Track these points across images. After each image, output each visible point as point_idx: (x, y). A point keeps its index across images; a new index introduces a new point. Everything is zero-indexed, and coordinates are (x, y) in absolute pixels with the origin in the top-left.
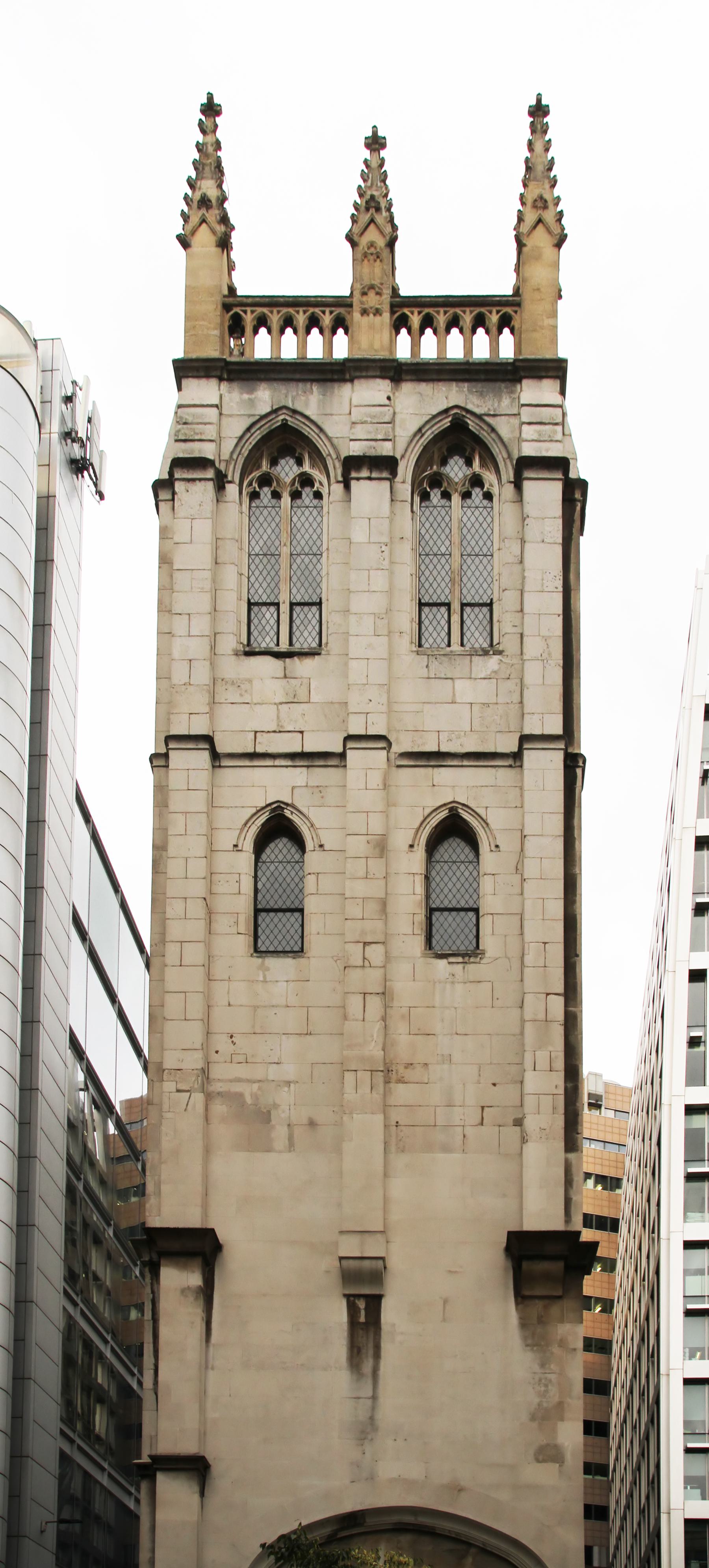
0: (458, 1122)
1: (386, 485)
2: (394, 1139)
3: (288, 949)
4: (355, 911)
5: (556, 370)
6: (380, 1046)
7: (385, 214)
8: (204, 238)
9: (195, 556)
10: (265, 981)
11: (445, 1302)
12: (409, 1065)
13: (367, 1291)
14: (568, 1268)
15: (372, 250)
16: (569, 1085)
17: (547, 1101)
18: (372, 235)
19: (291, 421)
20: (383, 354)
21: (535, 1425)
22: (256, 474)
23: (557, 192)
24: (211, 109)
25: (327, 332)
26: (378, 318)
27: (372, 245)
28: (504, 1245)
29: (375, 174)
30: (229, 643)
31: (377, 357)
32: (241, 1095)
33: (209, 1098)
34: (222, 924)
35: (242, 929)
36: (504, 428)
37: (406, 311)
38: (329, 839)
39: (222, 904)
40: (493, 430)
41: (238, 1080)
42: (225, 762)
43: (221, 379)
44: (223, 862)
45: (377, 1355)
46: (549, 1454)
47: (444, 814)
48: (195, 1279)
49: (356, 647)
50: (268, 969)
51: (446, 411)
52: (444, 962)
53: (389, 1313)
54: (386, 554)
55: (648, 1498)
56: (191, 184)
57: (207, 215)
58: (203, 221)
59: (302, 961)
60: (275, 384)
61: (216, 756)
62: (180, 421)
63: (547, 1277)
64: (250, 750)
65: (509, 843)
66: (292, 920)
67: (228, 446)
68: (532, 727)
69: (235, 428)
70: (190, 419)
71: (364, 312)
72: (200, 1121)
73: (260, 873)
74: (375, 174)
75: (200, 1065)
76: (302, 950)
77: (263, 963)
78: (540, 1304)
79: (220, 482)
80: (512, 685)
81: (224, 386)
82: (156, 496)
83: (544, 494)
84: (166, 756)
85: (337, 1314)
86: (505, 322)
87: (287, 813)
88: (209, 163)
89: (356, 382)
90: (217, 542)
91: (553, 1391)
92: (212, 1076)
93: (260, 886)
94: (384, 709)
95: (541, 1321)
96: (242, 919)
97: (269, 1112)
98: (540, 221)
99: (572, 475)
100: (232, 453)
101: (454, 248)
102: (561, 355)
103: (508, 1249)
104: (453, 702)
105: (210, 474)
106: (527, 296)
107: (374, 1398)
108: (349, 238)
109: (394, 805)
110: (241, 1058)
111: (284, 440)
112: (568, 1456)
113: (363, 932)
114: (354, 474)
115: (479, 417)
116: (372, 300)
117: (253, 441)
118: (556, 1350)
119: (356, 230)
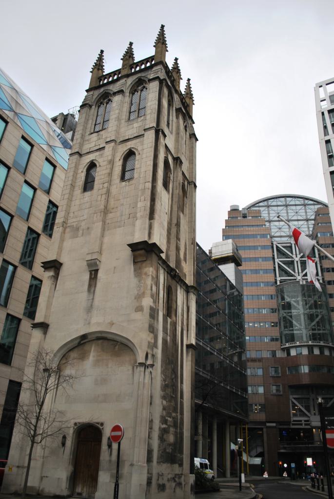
11: (115, 268)
12: (113, 208)
16: (152, 203)
35: (80, 188)
45: (95, 286)
46: (139, 309)
53: (100, 274)
78: (140, 263)
85: (87, 277)
91: (142, 288)
95: (140, 268)
96: (81, 186)
107: (93, 299)
112: (145, 309)
118: (144, 276)
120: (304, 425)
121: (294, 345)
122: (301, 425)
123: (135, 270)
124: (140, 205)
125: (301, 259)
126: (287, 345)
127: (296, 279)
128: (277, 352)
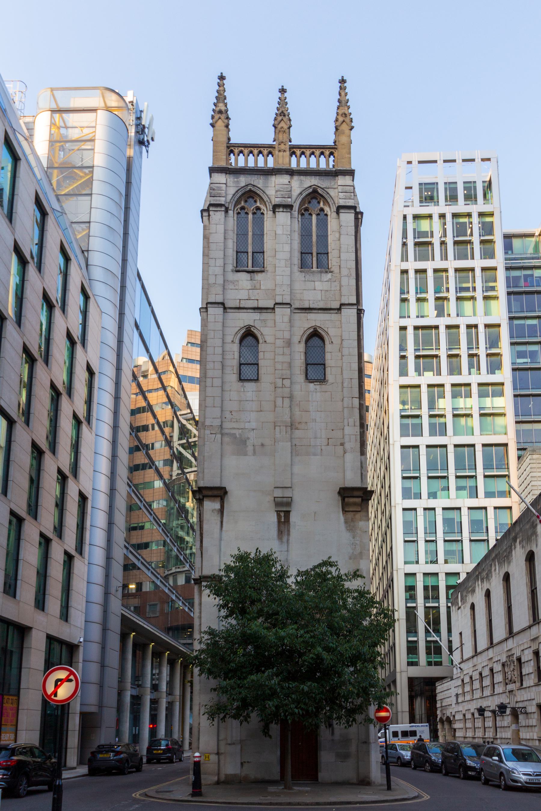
0: (318, 444)
1: (289, 214)
2: (295, 450)
3: (252, 378)
4: (279, 366)
5: (351, 173)
6: (289, 417)
7: (287, 117)
8: (220, 124)
9: (218, 237)
10: (244, 391)
11: (315, 513)
13: (284, 509)
14: (362, 500)
15: (282, 130)
16: (361, 430)
17: (353, 438)
18: (282, 124)
19: (253, 189)
20: (286, 167)
21: (351, 561)
22: (239, 206)
23: (350, 111)
24: (222, 78)
25: (265, 156)
26: (285, 153)
27: (282, 127)
28: (338, 491)
29: (282, 102)
30: (230, 267)
31: (284, 167)
32: (235, 434)
33: (222, 434)
34: (228, 370)
35: (235, 372)
36: (332, 193)
37: (295, 150)
38: (269, 339)
39: (228, 363)
40: (328, 193)
41: (234, 429)
42: (228, 310)
43: (226, 173)
44: (228, 347)
45: (289, 534)
47: (312, 330)
48: (217, 506)
49: (279, 271)
50: (245, 387)
51: (311, 186)
52: (313, 384)
53: (294, 518)
54: (289, 238)
55: (387, 562)
56: (215, 105)
57: (221, 115)
58: (220, 118)
59: (259, 384)
60: (247, 176)
61: (225, 308)
62: (211, 189)
63: (355, 504)
64: (238, 306)
65: (337, 341)
66: (254, 368)
67: (229, 197)
68: (345, 300)
69: (232, 191)
70: (216, 188)
71: (280, 151)
72: (220, 444)
73: (241, 351)
74: (282, 102)
75: (220, 424)
76: (258, 379)
77: (243, 385)
79: (227, 211)
80: (337, 283)
81: (227, 175)
82: (202, 214)
83: (348, 217)
84: (206, 308)
86: (332, 154)
87: (252, 329)
88: (221, 97)
89: (277, 176)
90: (225, 231)
92: (223, 427)
93: (241, 355)
94: (289, 293)
97: (246, 441)
98: (343, 120)
99: (358, 210)
100: (231, 200)
101: (312, 127)
102: (353, 168)
103: (339, 493)
104: (315, 290)
105: (223, 209)
106: (339, 146)
108: (274, 126)
109: (293, 327)
110: (235, 420)
111: (249, 195)
113: (282, 375)
114: (277, 210)
115: (323, 189)
116: (282, 147)
117: (238, 195)
119: (276, 123)
123: (346, 522)
124: (347, 430)
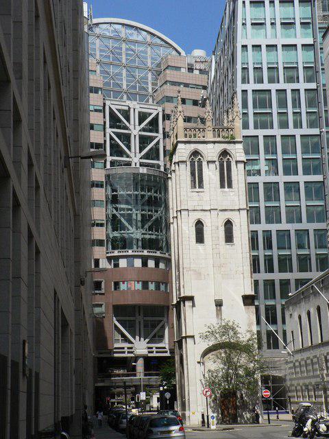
120: (126, 353)
121: (124, 254)
122: (124, 352)
125: (140, 133)
126: (116, 253)
127: (129, 164)
128: (101, 260)
